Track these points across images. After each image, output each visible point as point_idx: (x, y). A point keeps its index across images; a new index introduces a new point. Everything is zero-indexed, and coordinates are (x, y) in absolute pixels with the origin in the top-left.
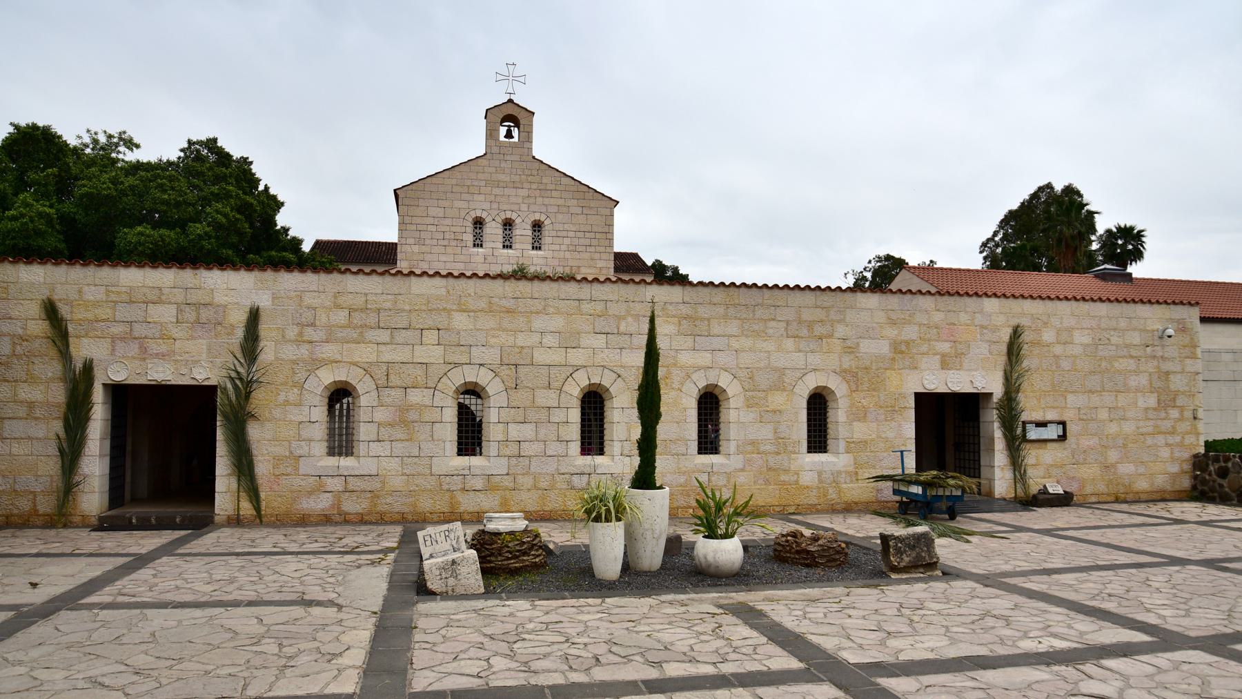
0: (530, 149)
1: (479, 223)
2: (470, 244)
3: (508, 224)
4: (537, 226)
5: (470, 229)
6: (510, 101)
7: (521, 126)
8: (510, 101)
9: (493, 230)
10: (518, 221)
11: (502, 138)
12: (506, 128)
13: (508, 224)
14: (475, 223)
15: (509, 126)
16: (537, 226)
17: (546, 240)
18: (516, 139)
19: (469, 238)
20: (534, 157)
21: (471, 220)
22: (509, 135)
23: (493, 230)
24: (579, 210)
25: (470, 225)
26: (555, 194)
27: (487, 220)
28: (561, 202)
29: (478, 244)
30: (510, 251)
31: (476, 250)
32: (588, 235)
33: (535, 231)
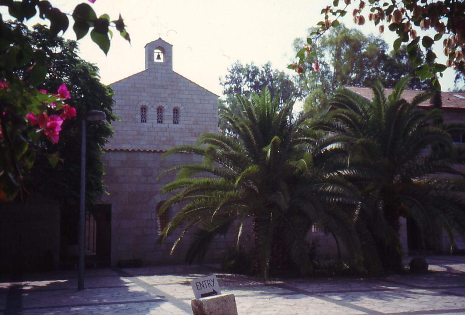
0: (171, 66)
1: (144, 109)
2: (139, 121)
3: (160, 110)
4: (176, 111)
5: (139, 112)
6: (160, 39)
7: (166, 53)
8: (160, 39)
9: (152, 113)
10: (166, 107)
11: (156, 60)
12: (158, 54)
13: (160, 110)
14: (142, 109)
15: (159, 53)
16: (176, 111)
17: (182, 118)
18: (162, 61)
19: (138, 117)
20: (173, 72)
21: (140, 107)
22: (159, 57)
23: (152, 113)
24: (198, 101)
25: (139, 109)
26: (186, 92)
27: (149, 107)
28: (189, 97)
29: (144, 120)
30: (161, 124)
31: (143, 124)
32: (204, 115)
33: (174, 113)
